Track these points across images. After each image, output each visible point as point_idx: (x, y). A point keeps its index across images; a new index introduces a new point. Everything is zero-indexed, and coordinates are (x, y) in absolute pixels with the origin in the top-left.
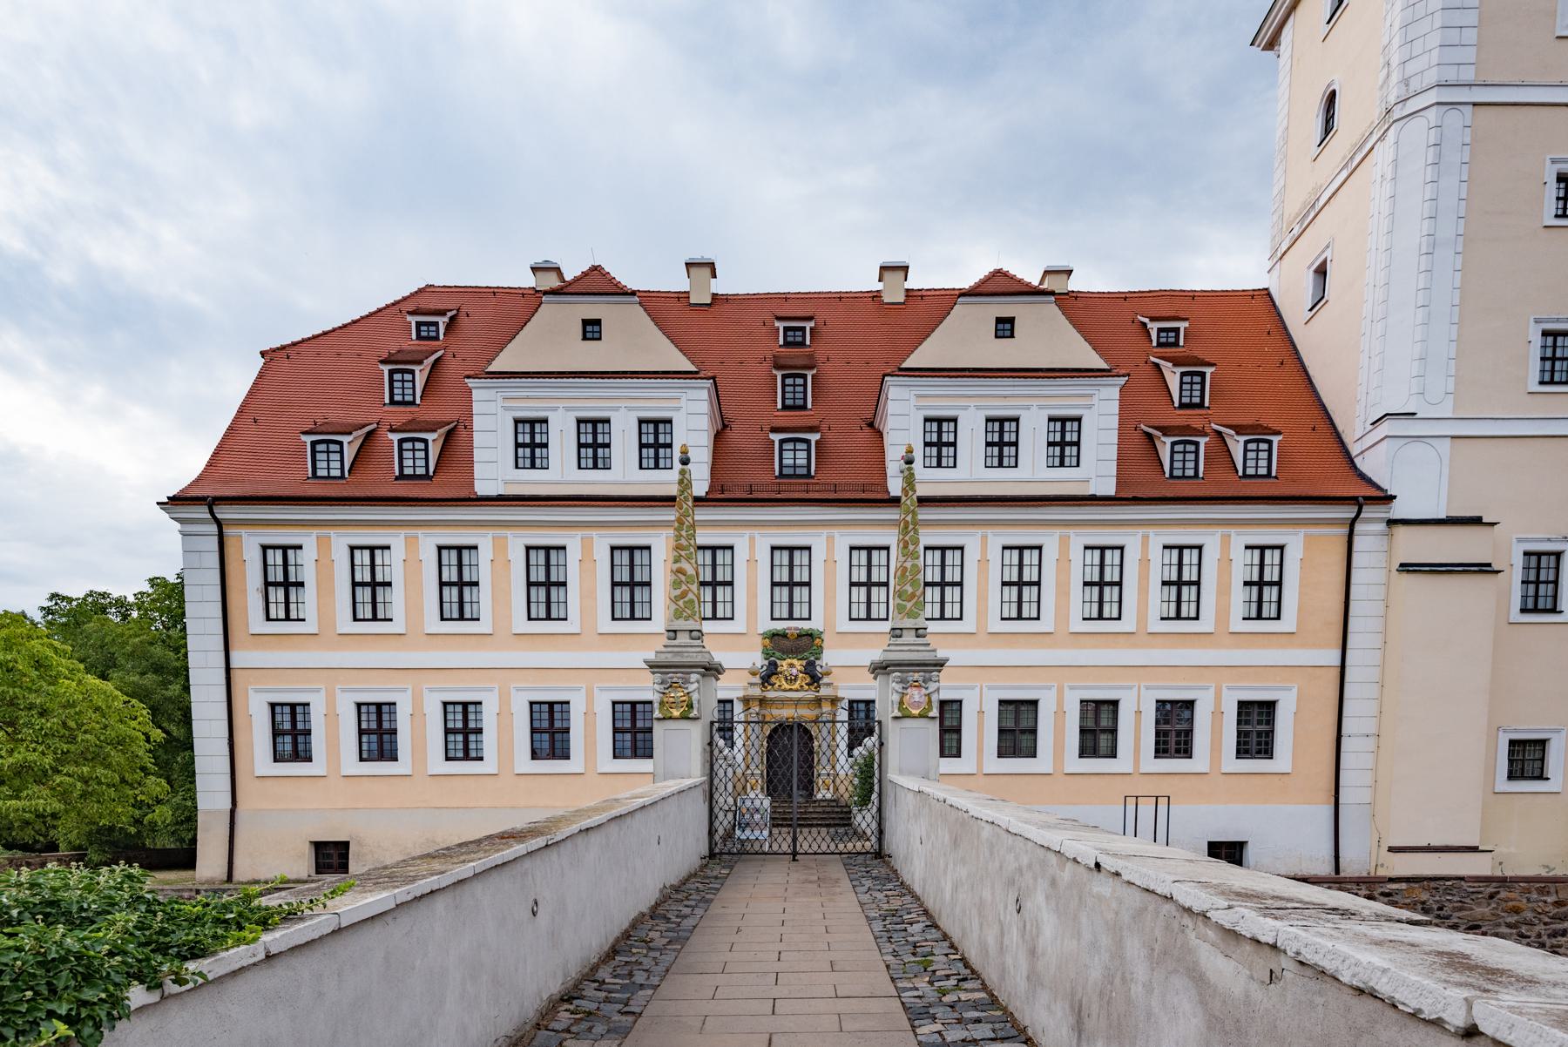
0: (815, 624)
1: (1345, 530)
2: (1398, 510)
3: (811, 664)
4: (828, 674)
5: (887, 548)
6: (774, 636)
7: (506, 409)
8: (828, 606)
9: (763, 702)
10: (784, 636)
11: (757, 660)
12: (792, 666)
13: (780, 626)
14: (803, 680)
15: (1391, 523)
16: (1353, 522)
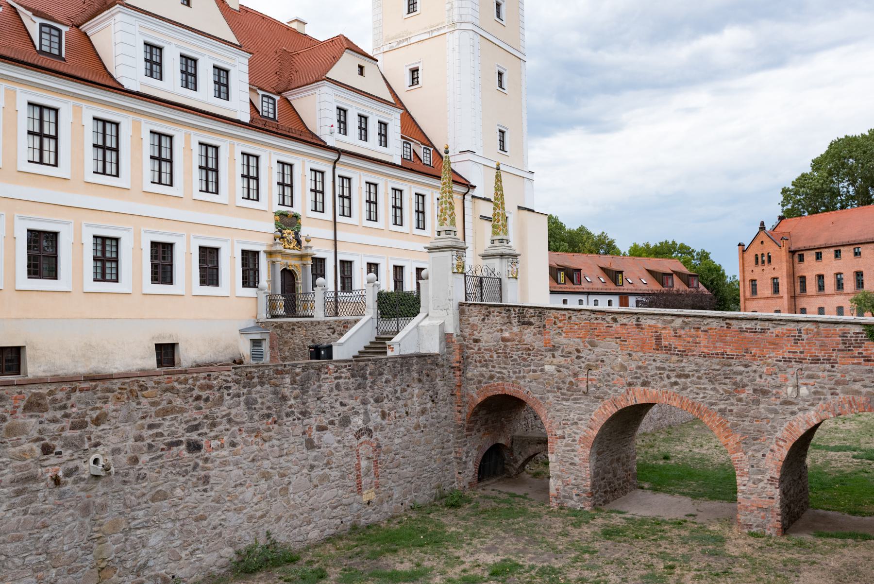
0: (296, 210)
1: (462, 197)
2: (476, 192)
3: (296, 234)
4: (308, 241)
5: (322, 173)
6: (283, 215)
7: (141, 33)
8: (302, 203)
9: (283, 255)
10: (286, 215)
11: (271, 227)
12: (288, 233)
13: (284, 209)
14: (295, 243)
15: (473, 197)
16: (465, 194)
